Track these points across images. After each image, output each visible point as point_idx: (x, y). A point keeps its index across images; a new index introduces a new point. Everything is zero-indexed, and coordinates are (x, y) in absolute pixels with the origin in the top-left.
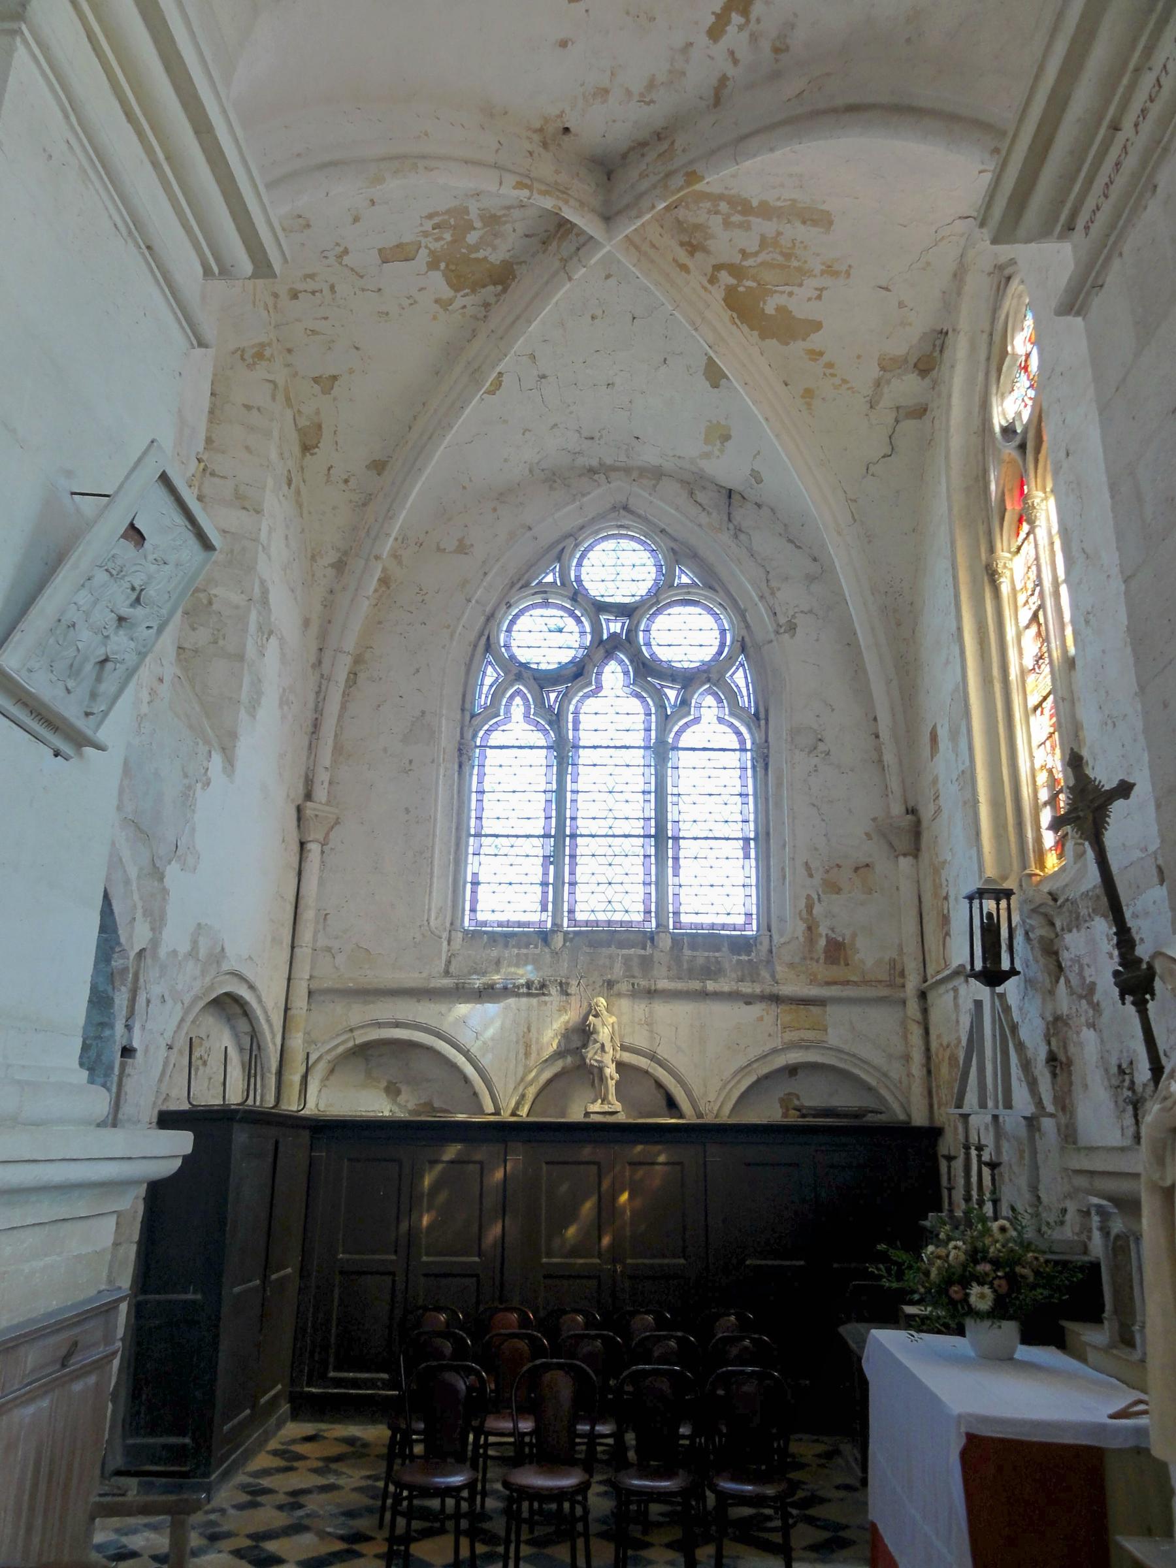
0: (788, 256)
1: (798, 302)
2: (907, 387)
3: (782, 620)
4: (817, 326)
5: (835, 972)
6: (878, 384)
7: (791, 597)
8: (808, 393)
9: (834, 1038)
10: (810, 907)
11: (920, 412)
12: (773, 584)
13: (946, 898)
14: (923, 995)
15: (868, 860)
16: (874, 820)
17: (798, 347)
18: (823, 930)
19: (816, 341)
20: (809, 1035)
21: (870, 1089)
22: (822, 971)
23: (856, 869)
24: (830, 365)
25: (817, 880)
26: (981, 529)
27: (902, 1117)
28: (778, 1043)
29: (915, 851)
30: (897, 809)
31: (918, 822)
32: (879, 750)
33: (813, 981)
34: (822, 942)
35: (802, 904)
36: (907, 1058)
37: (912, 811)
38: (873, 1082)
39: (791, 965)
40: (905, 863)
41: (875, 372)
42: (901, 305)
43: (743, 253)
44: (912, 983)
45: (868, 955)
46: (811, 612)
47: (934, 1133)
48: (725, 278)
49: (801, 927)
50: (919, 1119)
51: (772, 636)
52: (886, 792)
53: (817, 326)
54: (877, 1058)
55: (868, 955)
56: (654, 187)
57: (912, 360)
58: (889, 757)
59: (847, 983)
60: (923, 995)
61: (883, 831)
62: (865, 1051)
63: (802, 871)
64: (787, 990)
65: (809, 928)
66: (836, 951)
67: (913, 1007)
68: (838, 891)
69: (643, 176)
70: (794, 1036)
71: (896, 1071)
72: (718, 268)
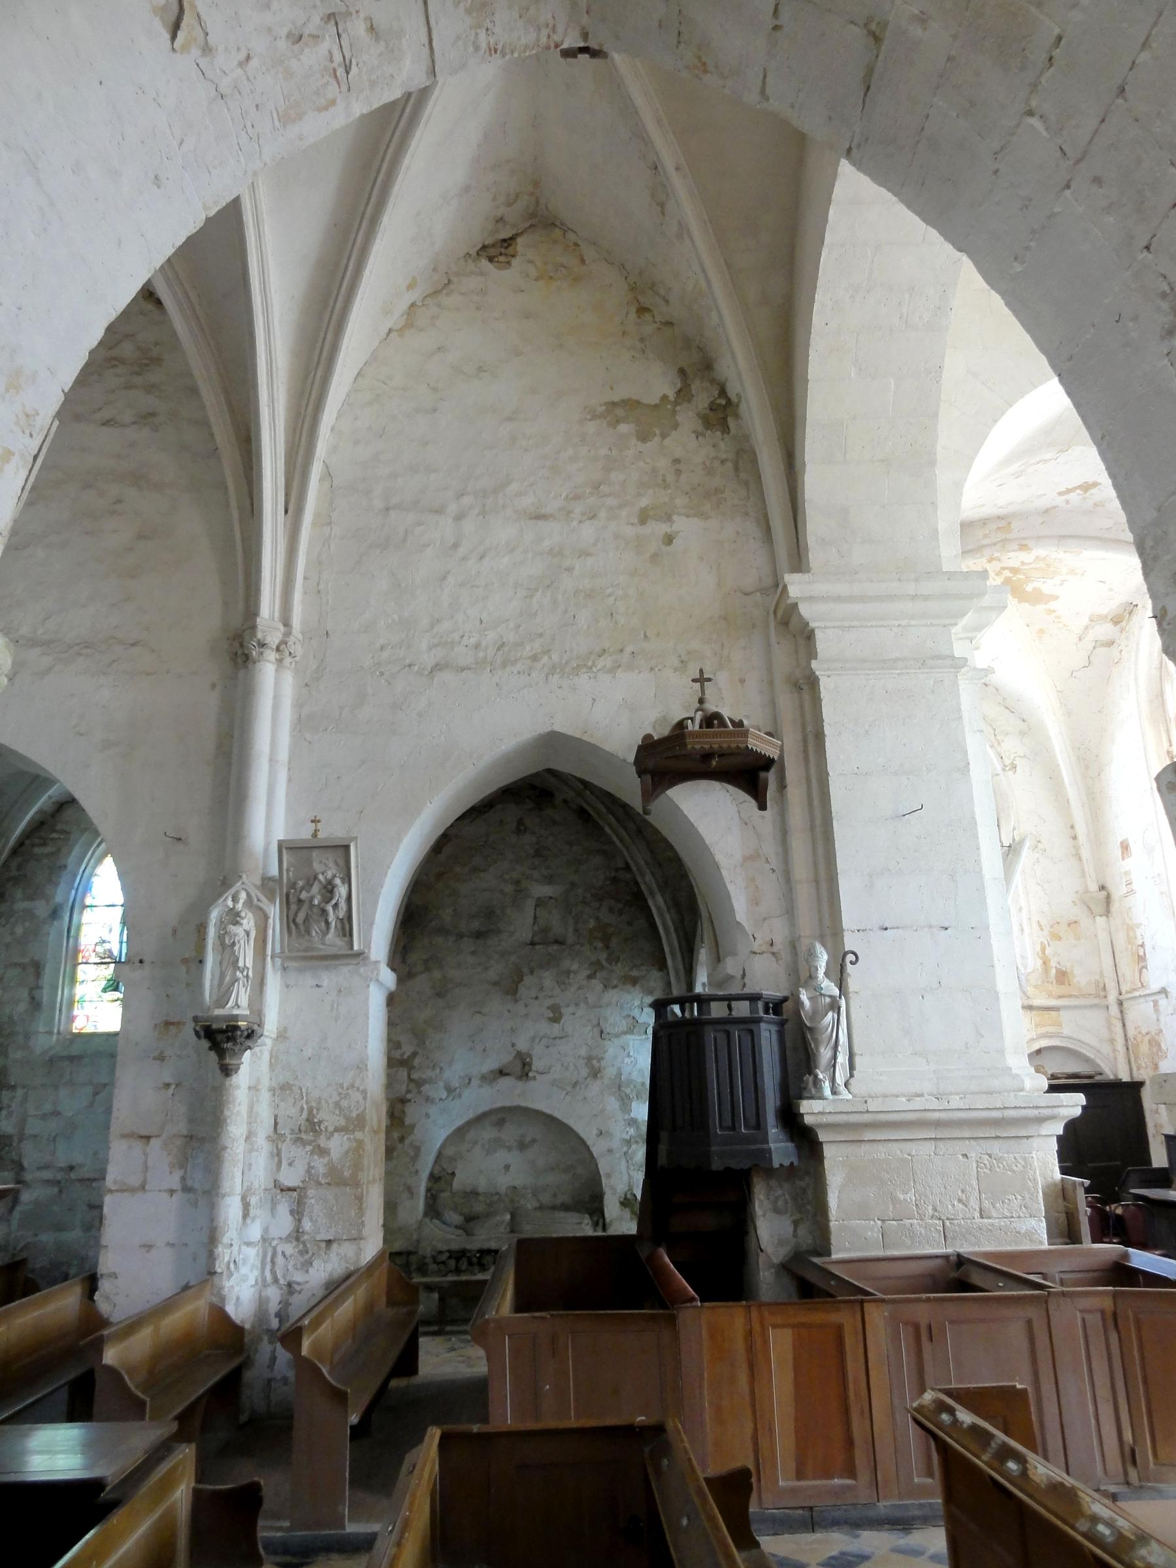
0: (1049, 566)
1: (1047, 587)
2: (1105, 630)
3: (1007, 762)
4: (1056, 598)
5: (1063, 990)
6: (1086, 628)
7: (1012, 746)
8: (1041, 631)
9: (1066, 1031)
10: (1043, 950)
11: (1110, 643)
12: (999, 737)
13: (1142, 946)
14: (1121, 1003)
15: (1075, 919)
16: (1077, 892)
17: (1041, 608)
18: (1053, 964)
19: (1052, 605)
20: (1051, 1029)
21: (1087, 1060)
22: (1056, 989)
23: (1069, 925)
24: (1059, 617)
25: (1046, 932)
26: (1162, 728)
27: (1112, 1077)
28: (1033, 1035)
29: (1107, 912)
30: (1093, 887)
31: (1108, 898)
32: (1077, 848)
33: (1050, 995)
34: (1054, 971)
35: (1038, 948)
36: (1112, 1041)
37: (1102, 888)
38: (1092, 1056)
39: (1036, 986)
40: (1101, 921)
41: (1086, 621)
42: (1111, 590)
43: (1023, 563)
44: (1112, 997)
45: (1082, 978)
46: (1025, 756)
47: (1135, 1087)
48: (1007, 573)
49: (1039, 962)
50: (1125, 1078)
51: (1000, 772)
52: (1083, 875)
53: (1056, 598)
54: (1094, 1042)
55: (1082, 978)
56: (994, 544)
57: (1109, 617)
58: (1085, 853)
59: (1070, 996)
60: (1121, 1003)
61: (1085, 902)
62: (1086, 1038)
63: (1035, 926)
64: (1037, 1002)
65: (1044, 963)
66: (1062, 976)
67: (1114, 1010)
68: (1060, 939)
69: (985, 536)
70: (1041, 1030)
71: (1106, 1049)
72: (1004, 569)
